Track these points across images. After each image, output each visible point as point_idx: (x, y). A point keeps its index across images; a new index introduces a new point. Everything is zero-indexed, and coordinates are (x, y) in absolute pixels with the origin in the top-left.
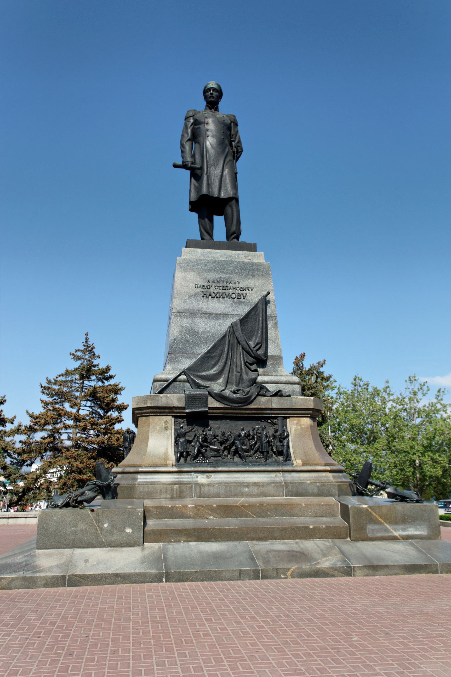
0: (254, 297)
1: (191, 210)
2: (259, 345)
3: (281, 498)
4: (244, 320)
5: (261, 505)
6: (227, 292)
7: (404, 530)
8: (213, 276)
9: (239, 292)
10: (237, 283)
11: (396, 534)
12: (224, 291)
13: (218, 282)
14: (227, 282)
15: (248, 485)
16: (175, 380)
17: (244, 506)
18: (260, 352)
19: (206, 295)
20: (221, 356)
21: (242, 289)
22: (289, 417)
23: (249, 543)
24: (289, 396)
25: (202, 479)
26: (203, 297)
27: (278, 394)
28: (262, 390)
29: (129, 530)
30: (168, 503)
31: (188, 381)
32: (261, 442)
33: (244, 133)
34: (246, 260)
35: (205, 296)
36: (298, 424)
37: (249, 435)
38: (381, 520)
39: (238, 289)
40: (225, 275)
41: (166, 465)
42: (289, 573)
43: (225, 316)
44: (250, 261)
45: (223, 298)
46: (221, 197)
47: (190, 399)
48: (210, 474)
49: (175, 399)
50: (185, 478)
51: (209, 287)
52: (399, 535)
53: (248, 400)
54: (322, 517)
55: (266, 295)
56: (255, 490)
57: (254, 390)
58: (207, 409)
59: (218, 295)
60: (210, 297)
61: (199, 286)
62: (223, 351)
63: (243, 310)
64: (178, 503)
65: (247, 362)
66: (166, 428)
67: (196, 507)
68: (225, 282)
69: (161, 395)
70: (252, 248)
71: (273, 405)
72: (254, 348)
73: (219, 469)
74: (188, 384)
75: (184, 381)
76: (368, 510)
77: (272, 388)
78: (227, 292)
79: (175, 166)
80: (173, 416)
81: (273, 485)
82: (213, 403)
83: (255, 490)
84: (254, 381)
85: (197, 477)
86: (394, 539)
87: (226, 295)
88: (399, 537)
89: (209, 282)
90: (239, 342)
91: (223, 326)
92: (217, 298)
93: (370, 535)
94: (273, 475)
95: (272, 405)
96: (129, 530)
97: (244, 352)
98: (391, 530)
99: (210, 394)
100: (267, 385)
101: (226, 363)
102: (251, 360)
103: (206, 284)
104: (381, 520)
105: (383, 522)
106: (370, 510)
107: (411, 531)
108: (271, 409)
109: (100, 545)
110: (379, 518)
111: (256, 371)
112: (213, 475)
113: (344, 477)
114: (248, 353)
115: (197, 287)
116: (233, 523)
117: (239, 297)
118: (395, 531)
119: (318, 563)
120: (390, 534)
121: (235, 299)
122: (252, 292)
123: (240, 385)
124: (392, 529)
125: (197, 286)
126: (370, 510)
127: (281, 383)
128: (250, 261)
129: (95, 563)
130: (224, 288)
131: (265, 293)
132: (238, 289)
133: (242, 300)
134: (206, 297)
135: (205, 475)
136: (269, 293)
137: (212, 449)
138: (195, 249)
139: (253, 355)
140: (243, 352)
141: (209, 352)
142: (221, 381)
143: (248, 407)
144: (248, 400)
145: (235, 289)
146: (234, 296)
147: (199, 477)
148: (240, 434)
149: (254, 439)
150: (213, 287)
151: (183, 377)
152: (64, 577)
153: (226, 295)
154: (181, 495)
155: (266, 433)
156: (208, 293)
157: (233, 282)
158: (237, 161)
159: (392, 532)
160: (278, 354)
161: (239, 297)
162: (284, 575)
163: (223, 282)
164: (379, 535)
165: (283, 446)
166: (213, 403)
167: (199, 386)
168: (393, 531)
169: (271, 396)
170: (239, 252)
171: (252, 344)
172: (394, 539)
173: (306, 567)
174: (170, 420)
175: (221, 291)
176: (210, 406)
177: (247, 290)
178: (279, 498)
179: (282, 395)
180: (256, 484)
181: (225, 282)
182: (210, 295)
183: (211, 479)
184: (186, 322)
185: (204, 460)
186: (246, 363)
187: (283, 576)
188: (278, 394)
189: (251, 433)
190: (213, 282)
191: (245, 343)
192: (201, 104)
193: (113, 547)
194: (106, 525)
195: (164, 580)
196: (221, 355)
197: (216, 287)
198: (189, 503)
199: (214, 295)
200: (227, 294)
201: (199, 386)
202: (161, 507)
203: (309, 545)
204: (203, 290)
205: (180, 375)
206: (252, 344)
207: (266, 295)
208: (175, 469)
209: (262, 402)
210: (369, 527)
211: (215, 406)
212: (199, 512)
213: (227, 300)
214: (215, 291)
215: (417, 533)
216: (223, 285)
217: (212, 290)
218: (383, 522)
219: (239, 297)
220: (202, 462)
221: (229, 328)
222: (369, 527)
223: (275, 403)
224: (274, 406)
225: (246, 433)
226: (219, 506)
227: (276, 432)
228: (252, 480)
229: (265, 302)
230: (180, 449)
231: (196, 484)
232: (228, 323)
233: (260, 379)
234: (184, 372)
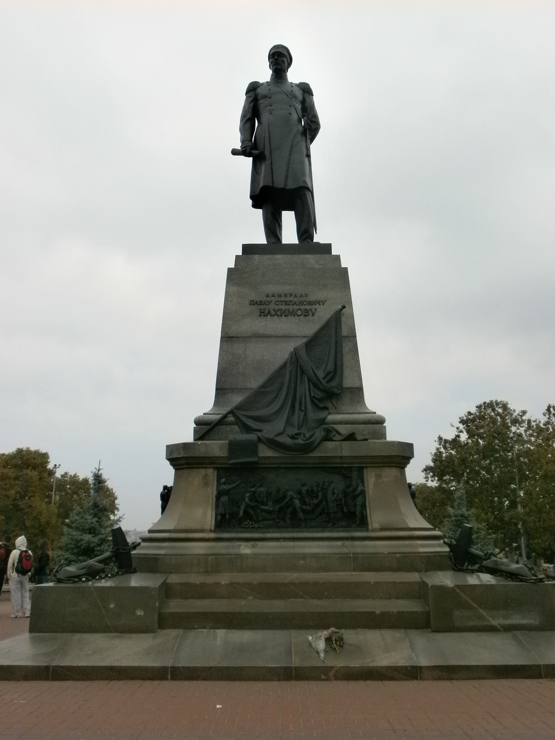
0: (324, 314)
1: (255, 206)
2: (331, 375)
3: (347, 573)
4: (311, 343)
5: (316, 584)
6: (291, 307)
7: (506, 617)
9: (307, 307)
10: (304, 295)
11: (495, 623)
12: (287, 307)
13: (280, 296)
14: (291, 295)
15: (304, 557)
16: (221, 422)
17: (293, 584)
18: (334, 384)
19: (263, 314)
20: (280, 391)
21: (310, 303)
22: (366, 467)
23: (294, 633)
24: (366, 440)
25: (245, 549)
26: (260, 316)
27: (351, 437)
29: (140, 613)
30: (196, 579)
31: (236, 424)
32: (327, 502)
33: (321, 104)
34: (317, 266)
35: (263, 314)
36: (378, 476)
37: (313, 491)
38: (473, 604)
39: (305, 303)
40: (288, 287)
41: (202, 531)
42: (331, 674)
44: (321, 266)
45: (285, 316)
46: (288, 188)
47: (234, 447)
48: (257, 543)
49: (216, 447)
51: (267, 303)
52: (499, 625)
53: (308, 448)
54: (397, 598)
55: (341, 310)
57: (319, 434)
58: (256, 459)
59: (279, 313)
60: (269, 315)
61: (255, 302)
62: (282, 384)
64: (210, 579)
65: (314, 397)
66: (206, 484)
67: (232, 584)
68: (288, 296)
69: (199, 442)
71: (344, 452)
72: (324, 378)
73: (269, 535)
74: (236, 427)
75: (232, 424)
76: (455, 590)
77: (344, 430)
78: (291, 307)
79: (235, 152)
80: (214, 468)
81: (337, 556)
82: (265, 452)
84: (323, 421)
85: (240, 546)
86: (492, 629)
87: (289, 312)
88: (498, 627)
89: (267, 296)
90: (303, 372)
92: (278, 316)
93: (458, 624)
94: (339, 543)
95: (342, 452)
96: (140, 613)
97: (311, 384)
98: (488, 617)
99: (259, 439)
100: (339, 428)
101: (286, 399)
102: (319, 394)
103: (264, 299)
104: (473, 604)
105: (475, 606)
106: (458, 590)
107: (516, 620)
108: (341, 457)
109: (105, 629)
110: (471, 601)
111: (326, 408)
112: (260, 544)
113: (439, 545)
114: (315, 385)
115: (253, 303)
116: (277, 606)
118: (493, 619)
119: (373, 661)
120: (485, 623)
121: (302, 317)
122: (324, 306)
123: (304, 427)
124: (489, 616)
125: (252, 303)
126: (458, 590)
127: (358, 424)
128: (321, 266)
129: (90, 652)
130: (286, 303)
131: (340, 307)
132: (305, 303)
133: (310, 317)
134: (264, 316)
135: (250, 544)
136: (344, 307)
137: (263, 511)
138: (251, 256)
139: (322, 388)
140: (309, 385)
141: (263, 386)
143: (311, 455)
144: (308, 448)
145: (301, 303)
146: (299, 313)
147: (242, 547)
148: (301, 490)
149: (317, 497)
150: (273, 303)
151: (231, 419)
152: (47, 668)
153: (289, 312)
155: (333, 489)
156: (267, 311)
157: (299, 295)
158: (312, 140)
159: (489, 621)
160: (357, 385)
161: (307, 314)
162: (325, 675)
163: (286, 295)
164: (471, 624)
165: (355, 505)
166: (265, 452)
168: (491, 619)
169: (341, 441)
170: (308, 256)
171: (321, 374)
174: (211, 473)
175: (284, 307)
176: (261, 454)
177: (318, 305)
178: (344, 573)
179: (355, 440)
180: (315, 556)
181: (288, 296)
182: (269, 313)
183: (256, 550)
185: (252, 525)
186: (312, 399)
187: (323, 677)
188: (351, 437)
189: (315, 489)
190: (273, 296)
191: (311, 371)
193: (121, 632)
194: (112, 606)
195: (169, 677)
196: (280, 389)
197: (277, 303)
198: (224, 579)
199: (273, 313)
200: (291, 311)
202: (187, 584)
204: (260, 307)
205: (225, 416)
206: (321, 374)
207: (341, 310)
208: (212, 535)
209: (331, 449)
210: (457, 613)
211: (268, 455)
212: (235, 591)
214: (276, 308)
215: (525, 622)
216: (286, 299)
217: (272, 306)
218: (475, 606)
219: (307, 314)
220: (249, 528)
221: (291, 354)
222: (457, 613)
223: (347, 450)
224: (345, 453)
225: (308, 490)
226: (260, 584)
227: (348, 487)
230: (221, 510)
231: (237, 555)
232: (289, 347)
233: (330, 418)
234: (231, 412)
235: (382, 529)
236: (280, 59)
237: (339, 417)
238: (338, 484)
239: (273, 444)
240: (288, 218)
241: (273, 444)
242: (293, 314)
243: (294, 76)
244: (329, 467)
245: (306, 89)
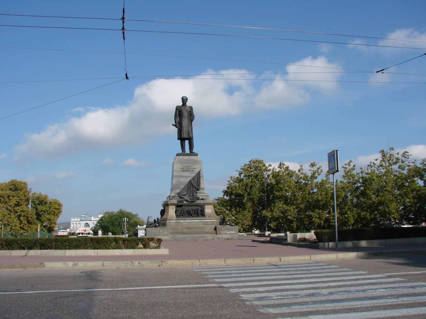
1: (178, 139)
8: (185, 165)
19: (183, 171)
25: (182, 221)
27: (203, 199)
28: (198, 199)
43: (188, 177)
50: (178, 221)
53: (194, 202)
56: (196, 224)
63: (194, 175)
70: (196, 155)
77: (201, 197)
79: (173, 125)
83: (196, 224)
91: (188, 180)
100: (200, 197)
107: (231, 232)
115: (180, 168)
117: (192, 171)
141: (184, 188)
142: (187, 196)
154: (177, 225)
166: (185, 202)
167: (182, 198)
172: (227, 234)
173: (204, 239)
174: (174, 207)
180: (196, 222)
184: (177, 179)
188: (203, 199)
192: (181, 104)
201: (182, 198)
203: (207, 235)
209: (198, 202)
210: (221, 231)
213: (189, 172)
217: (185, 169)
223: (202, 202)
228: (195, 221)
229: (199, 173)
235: (209, 217)
236: (184, 100)
237: (200, 195)
238: (200, 208)
239: (187, 201)
240: (187, 142)
241: (187, 201)
242: (190, 171)
243: (188, 104)
244: (197, 205)
245: (191, 108)
